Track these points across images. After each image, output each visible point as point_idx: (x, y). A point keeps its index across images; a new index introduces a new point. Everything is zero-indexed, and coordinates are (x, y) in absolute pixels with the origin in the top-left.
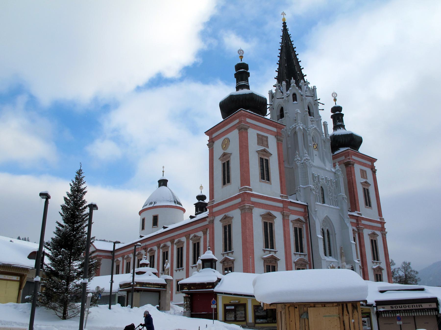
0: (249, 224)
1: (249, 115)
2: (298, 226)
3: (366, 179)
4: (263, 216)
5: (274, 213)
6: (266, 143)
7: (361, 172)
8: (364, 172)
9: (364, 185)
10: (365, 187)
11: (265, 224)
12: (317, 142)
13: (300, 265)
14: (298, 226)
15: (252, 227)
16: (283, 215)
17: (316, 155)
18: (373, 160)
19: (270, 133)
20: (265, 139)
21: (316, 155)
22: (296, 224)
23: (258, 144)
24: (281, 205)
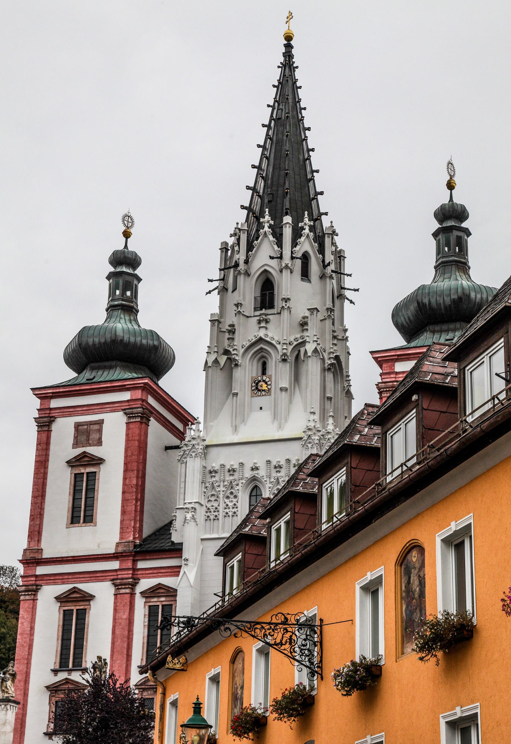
0: (25, 624)
1: (53, 393)
4: (61, 599)
5: (86, 587)
6: (97, 436)
11: (67, 616)
13: (152, 692)
14: (160, 601)
16: (115, 585)
17: (261, 408)
19: (108, 409)
20: (96, 427)
21: (261, 408)
22: (155, 599)
23: (76, 444)
24: (115, 565)
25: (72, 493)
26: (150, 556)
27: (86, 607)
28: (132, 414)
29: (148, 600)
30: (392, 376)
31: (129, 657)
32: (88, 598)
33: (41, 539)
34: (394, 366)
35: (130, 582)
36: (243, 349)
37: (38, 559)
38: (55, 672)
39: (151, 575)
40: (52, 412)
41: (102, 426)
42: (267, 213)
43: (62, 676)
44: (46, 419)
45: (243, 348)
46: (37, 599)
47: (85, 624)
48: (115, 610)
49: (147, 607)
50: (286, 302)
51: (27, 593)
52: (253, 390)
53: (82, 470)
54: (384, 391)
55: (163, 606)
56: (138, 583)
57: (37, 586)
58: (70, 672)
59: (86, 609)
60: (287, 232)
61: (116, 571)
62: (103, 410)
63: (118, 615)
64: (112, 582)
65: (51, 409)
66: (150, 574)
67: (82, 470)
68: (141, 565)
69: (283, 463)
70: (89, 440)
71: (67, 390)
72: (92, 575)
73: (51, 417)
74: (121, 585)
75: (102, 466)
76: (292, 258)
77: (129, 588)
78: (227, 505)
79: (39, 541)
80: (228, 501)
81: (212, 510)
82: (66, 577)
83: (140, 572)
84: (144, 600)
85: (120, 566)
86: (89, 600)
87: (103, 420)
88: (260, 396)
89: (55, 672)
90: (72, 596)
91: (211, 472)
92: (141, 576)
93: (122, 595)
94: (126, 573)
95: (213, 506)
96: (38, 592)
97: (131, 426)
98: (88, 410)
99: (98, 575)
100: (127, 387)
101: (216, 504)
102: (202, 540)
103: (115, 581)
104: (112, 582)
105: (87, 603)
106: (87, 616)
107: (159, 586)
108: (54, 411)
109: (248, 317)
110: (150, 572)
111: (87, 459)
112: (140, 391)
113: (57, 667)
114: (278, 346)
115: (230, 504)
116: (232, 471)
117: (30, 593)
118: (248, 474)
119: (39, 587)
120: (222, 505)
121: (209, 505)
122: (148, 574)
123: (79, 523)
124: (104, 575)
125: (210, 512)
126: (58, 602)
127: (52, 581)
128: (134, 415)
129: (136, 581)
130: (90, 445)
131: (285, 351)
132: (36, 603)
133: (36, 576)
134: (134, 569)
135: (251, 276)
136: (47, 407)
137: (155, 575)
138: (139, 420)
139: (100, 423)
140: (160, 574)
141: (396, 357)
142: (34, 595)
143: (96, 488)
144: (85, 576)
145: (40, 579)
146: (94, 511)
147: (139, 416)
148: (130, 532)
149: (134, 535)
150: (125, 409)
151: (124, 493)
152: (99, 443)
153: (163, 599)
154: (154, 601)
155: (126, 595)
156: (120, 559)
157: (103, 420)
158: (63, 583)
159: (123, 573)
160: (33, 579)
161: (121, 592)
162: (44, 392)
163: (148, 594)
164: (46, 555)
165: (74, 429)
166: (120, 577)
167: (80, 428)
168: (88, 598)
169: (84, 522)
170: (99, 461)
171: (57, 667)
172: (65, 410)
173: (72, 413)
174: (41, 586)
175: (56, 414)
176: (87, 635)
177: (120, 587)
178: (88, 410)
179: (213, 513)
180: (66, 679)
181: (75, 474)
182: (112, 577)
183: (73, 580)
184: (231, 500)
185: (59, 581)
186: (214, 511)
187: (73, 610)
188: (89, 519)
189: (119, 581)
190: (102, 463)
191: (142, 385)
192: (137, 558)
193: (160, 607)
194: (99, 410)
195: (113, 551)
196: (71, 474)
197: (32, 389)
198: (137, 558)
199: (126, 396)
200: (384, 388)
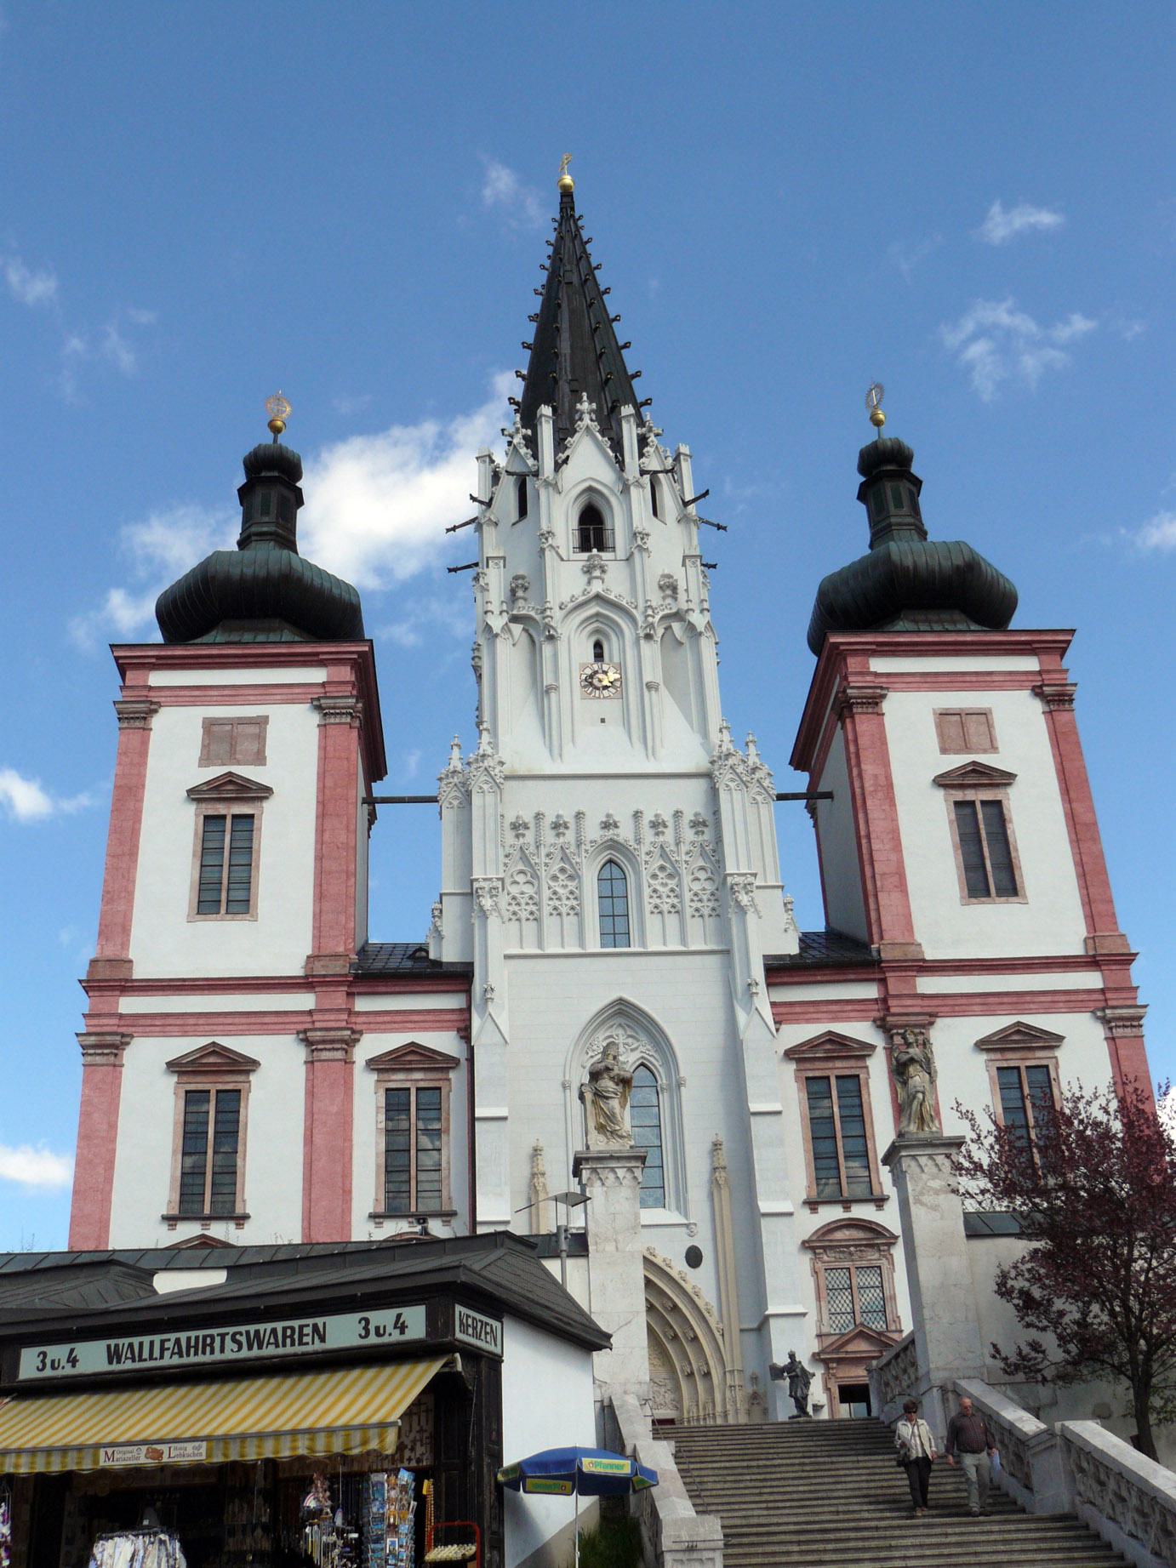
1: (157, 657)
2: (417, 1080)
3: (985, 751)
6: (255, 747)
7: (940, 727)
8: (973, 725)
9: (962, 787)
10: (970, 795)
12: (616, 659)
15: (113, 1127)
16: (308, 1042)
18: (1052, 644)
19: (278, 697)
20: (253, 730)
21: (603, 721)
22: (401, 1076)
23: (206, 759)
24: (304, 1001)
25: (200, 854)
26: (386, 986)
27: (239, 1086)
28: (334, 708)
29: (386, 1076)
30: (869, 678)
31: (347, 1193)
32: (244, 1066)
33: (128, 941)
34: (868, 663)
35: (346, 1038)
36: (564, 612)
37: (127, 980)
38: (171, 1220)
39: (388, 1026)
40: (152, 694)
41: (265, 728)
42: (585, 398)
43: (189, 1230)
44: (142, 705)
45: (561, 608)
46: (122, 1066)
47: (238, 1122)
48: (311, 1093)
49: (382, 1093)
50: (642, 539)
51: (100, 1051)
52: (585, 687)
53: (221, 809)
54: (858, 703)
55: (418, 1089)
56: (358, 1040)
57: (123, 1035)
58: (208, 1222)
59: (239, 1091)
60: (630, 433)
61: (310, 1013)
62: (267, 698)
63: (317, 1105)
64: (301, 1036)
65: (150, 688)
66: (385, 1023)
67: (221, 809)
68: (363, 1004)
69: (667, 817)
70: (235, 753)
71: (192, 653)
72: (253, 1020)
73: (152, 703)
74: (324, 1042)
75: (265, 804)
76: (643, 473)
77: (344, 1049)
78: (555, 893)
79: (125, 945)
80: (556, 884)
81: (523, 902)
82: (192, 1021)
83: (360, 1019)
84: (374, 1076)
85: (317, 1003)
86: (248, 1072)
87: (267, 717)
88: (599, 698)
89: (171, 1220)
90: (205, 1061)
91: (515, 826)
92: (364, 1027)
93: (326, 1064)
94: (332, 1017)
95: (522, 893)
96: (124, 1049)
97: (331, 731)
98: (235, 696)
99: (267, 1020)
100: (321, 657)
101: (529, 890)
102: (507, 957)
103: (309, 1034)
104: (301, 1036)
105: (241, 1078)
106: (242, 1104)
107: (413, 1049)
108: (158, 694)
109: (562, 560)
110: (386, 1019)
111: (230, 787)
112: (348, 668)
113: (175, 1212)
114: (634, 611)
115: (561, 891)
116: (558, 826)
117: (106, 1051)
118: (593, 832)
119: (127, 1039)
120: (546, 893)
121: (514, 890)
122: (382, 1023)
123: (218, 913)
124: (280, 1020)
125: (518, 904)
126: (173, 1072)
127: (158, 1029)
128: (338, 711)
129: (356, 1036)
130: (239, 763)
131: (650, 619)
132: (121, 1073)
133: (121, 1016)
134: (350, 1012)
135: (563, 495)
136: (141, 684)
137: (396, 1026)
138: (349, 720)
139: (262, 722)
140: (409, 1025)
141: (874, 647)
142: (116, 1055)
143: (255, 846)
144: (237, 1020)
145: (128, 1022)
146: (253, 890)
147: (351, 714)
148: (337, 936)
149: (345, 943)
150: (318, 699)
151: (319, 858)
152: (260, 759)
153: (418, 1075)
154: (399, 1080)
155: (336, 1063)
156: (317, 989)
157: (267, 717)
158: (185, 1034)
159: (326, 1017)
160: (114, 1021)
161: (323, 1058)
162: (139, 654)
163: (379, 1065)
164: (140, 972)
165: (200, 731)
166: (318, 1025)
167: (215, 728)
168: (244, 1066)
169: (227, 913)
170: (262, 793)
171: (175, 1212)
172: (182, 693)
173: (198, 699)
174: (132, 1036)
175: (163, 699)
176: (245, 1144)
177: (320, 1047)
178: (235, 696)
179: (523, 906)
180: (203, 1236)
181: (206, 818)
182: (301, 1027)
183: (207, 1028)
184: (561, 883)
185: (176, 1028)
186: (527, 904)
187: (209, 1091)
188: (242, 905)
189: (319, 1033)
190: (266, 798)
191: (355, 656)
192: (354, 990)
193: (413, 1092)
194: (259, 698)
195: (301, 973)
196: (197, 815)
197: (112, 646)
198: (354, 990)
199: (317, 675)
200: (855, 698)
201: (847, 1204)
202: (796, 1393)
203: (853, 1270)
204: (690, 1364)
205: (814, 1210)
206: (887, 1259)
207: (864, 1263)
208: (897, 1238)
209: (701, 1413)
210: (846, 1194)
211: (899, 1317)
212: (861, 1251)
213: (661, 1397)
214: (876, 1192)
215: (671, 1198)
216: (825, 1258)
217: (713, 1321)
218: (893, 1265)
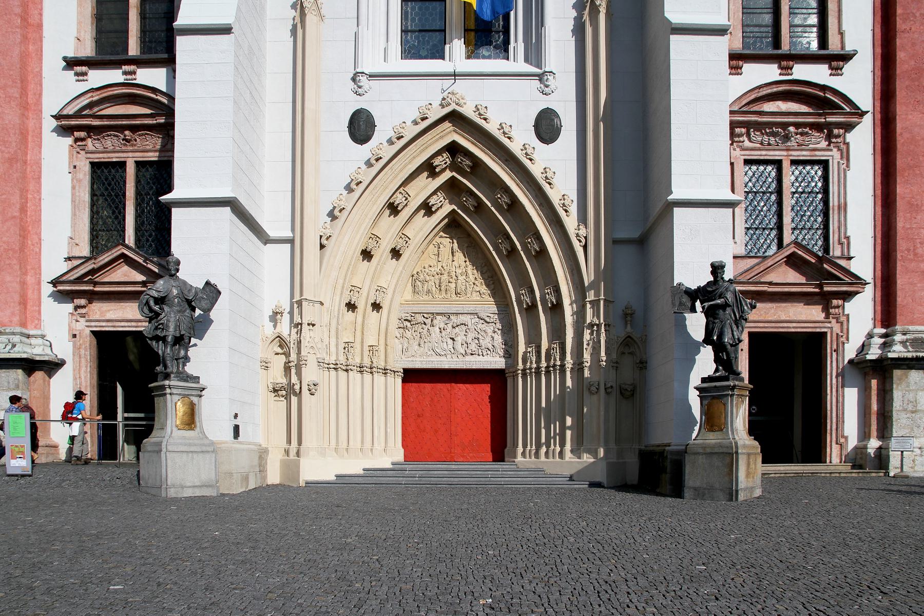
201: (786, 60)
202: (721, 335)
203: (786, 164)
204: (532, 291)
205: (735, 70)
206: (839, 149)
207: (804, 155)
208: (862, 114)
209: (544, 364)
210: (785, 47)
211: (848, 238)
212: (802, 134)
213: (488, 339)
214: (834, 45)
215: (517, 45)
216: (747, 144)
217: (571, 222)
218: (848, 160)
